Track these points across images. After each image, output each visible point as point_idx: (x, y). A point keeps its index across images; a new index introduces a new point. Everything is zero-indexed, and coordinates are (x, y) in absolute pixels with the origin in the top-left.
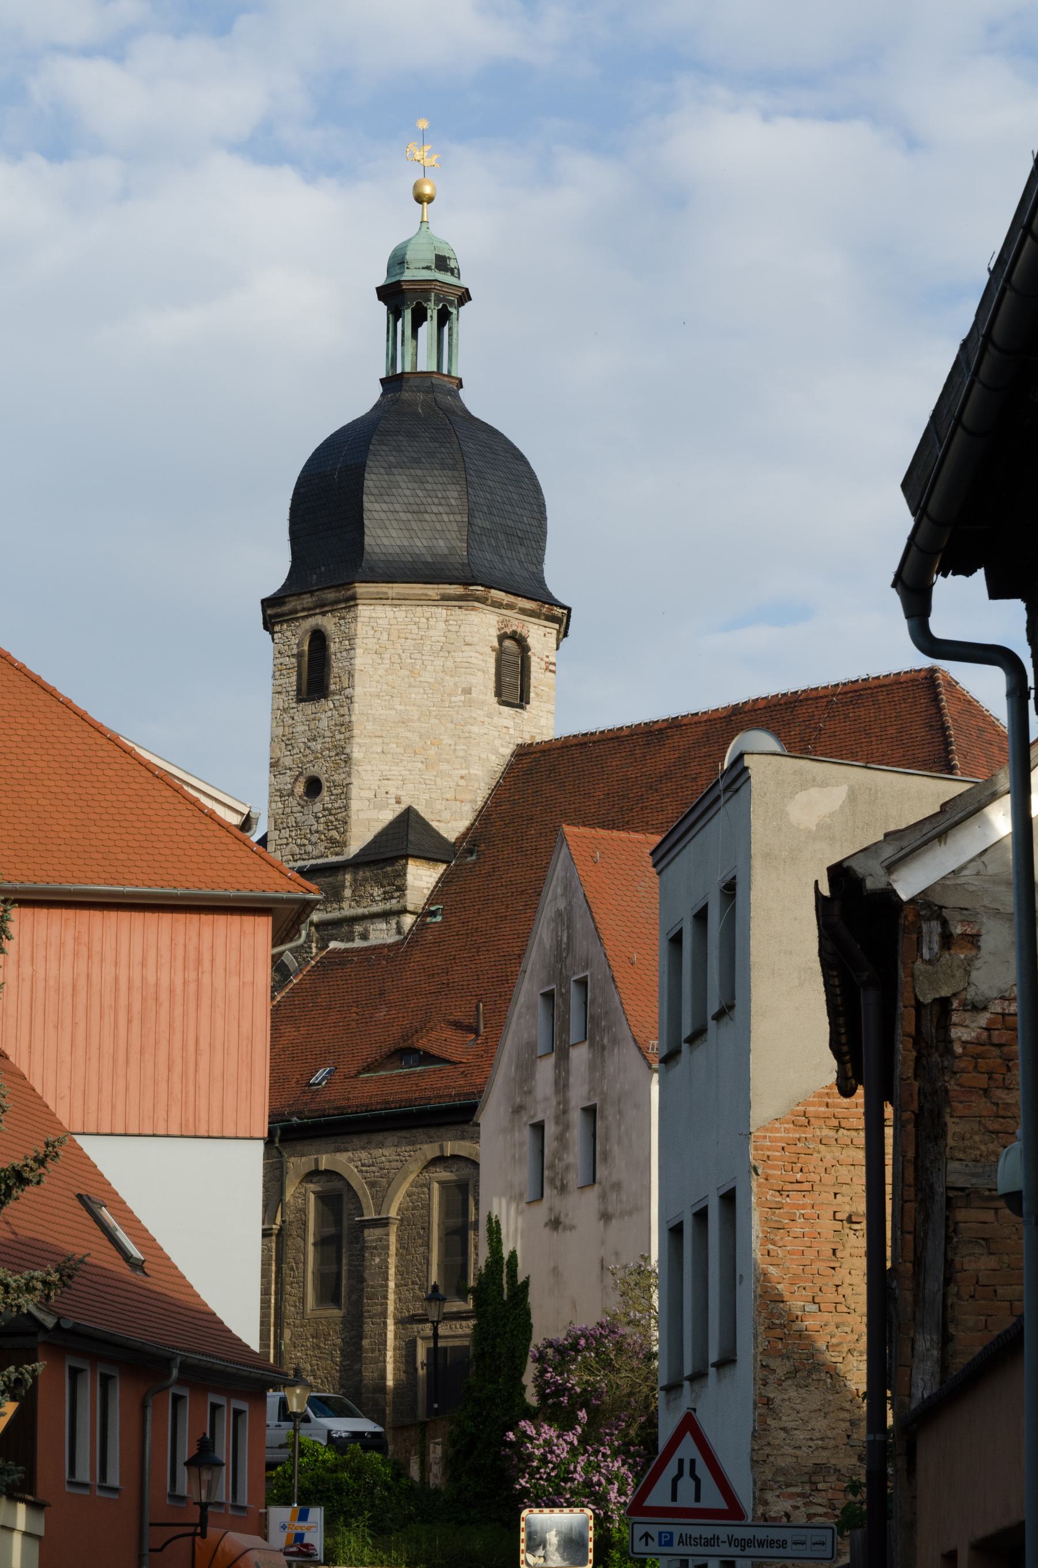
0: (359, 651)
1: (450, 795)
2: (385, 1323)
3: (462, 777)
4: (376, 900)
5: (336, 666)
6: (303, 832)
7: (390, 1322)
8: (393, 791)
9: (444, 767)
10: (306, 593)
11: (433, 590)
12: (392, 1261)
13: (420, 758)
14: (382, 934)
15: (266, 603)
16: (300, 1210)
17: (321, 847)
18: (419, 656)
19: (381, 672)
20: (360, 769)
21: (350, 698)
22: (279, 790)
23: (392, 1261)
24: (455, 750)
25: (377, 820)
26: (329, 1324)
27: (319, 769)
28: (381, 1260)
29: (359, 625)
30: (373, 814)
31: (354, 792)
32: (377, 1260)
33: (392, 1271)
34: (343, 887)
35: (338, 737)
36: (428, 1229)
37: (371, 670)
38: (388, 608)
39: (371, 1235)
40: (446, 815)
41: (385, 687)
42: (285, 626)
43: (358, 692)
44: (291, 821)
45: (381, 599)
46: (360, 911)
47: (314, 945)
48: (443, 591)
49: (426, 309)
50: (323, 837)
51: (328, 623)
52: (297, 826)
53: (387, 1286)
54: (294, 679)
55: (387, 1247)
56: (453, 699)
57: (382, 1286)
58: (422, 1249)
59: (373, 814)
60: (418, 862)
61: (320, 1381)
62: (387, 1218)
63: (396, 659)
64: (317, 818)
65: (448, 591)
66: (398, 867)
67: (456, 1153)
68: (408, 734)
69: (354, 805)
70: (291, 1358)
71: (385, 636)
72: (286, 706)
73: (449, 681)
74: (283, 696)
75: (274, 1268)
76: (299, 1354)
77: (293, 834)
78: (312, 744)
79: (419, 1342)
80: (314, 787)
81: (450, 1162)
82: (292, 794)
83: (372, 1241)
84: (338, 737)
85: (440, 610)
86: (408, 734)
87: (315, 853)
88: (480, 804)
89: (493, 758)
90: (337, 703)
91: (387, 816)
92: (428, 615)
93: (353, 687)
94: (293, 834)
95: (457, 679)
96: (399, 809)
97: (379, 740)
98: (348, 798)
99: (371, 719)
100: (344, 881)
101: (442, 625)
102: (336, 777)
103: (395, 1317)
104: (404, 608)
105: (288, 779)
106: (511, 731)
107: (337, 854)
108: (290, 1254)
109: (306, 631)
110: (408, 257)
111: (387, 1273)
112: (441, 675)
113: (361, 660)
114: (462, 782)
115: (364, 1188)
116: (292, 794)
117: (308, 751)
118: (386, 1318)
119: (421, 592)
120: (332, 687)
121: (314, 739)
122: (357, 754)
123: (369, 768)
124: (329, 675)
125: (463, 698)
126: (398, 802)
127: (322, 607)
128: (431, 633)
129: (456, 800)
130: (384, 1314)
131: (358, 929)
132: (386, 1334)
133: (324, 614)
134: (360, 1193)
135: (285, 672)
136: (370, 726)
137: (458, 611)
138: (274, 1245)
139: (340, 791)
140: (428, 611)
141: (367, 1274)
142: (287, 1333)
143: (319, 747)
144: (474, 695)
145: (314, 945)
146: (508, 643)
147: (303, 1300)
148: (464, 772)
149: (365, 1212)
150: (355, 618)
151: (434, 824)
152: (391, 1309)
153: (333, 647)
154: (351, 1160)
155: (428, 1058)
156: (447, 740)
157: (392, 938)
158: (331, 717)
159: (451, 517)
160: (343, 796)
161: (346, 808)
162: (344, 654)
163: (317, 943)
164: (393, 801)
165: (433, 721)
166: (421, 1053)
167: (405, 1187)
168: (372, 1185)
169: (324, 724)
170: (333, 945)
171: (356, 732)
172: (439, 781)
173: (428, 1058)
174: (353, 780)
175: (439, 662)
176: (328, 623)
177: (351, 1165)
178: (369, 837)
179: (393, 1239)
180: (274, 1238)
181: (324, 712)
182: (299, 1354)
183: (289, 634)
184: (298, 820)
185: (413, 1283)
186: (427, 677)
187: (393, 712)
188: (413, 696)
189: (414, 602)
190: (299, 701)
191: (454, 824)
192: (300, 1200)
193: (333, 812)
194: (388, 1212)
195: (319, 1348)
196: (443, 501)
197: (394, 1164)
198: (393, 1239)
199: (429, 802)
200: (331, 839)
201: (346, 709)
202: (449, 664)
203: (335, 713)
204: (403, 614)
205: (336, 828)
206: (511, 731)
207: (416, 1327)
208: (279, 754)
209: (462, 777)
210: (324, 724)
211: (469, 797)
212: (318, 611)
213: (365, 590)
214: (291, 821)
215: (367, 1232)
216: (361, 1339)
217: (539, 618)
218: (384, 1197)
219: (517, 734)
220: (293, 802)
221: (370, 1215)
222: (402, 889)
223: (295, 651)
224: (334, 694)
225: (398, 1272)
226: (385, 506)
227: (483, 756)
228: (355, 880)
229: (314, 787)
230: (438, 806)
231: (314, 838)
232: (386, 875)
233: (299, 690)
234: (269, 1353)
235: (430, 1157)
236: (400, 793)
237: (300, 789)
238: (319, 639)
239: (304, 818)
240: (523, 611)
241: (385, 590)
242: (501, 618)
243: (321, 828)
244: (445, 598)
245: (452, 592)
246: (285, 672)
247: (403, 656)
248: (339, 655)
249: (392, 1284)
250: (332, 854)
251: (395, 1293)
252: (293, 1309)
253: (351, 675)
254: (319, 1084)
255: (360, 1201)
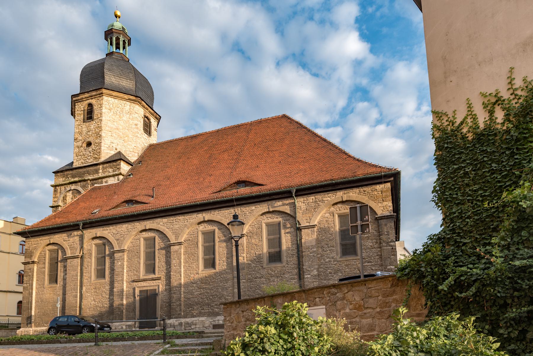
0: (104, 108)
1: (132, 150)
2: (123, 283)
3: (135, 146)
4: (111, 171)
5: (96, 112)
6: (85, 156)
7: (125, 282)
8: (114, 146)
9: (130, 143)
10: (86, 92)
11: (126, 97)
12: (125, 263)
13: (123, 139)
14: (112, 181)
15: (73, 96)
16: (89, 250)
17: (92, 160)
18: (122, 113)
19: (111, 115)
20: (104, 139)
21: (101, 120)
22: (77, 146)
23: (125, 263)
24: (133, 139)
25: (110, 153)
26: (100, 284)
27: (91, 139)
28: (121, 263)
29: (104, 101)
30: (109, 151)
31: (102, 144)
32: (120, 263)
33: (125, 267)
34: (99, 170)
35: (97, 130)
36: (139, 253)
37: (107, 114)
38: (113, 99)
39: (117, 255)
40: (130, 155)
41: (112, 119)
42: (79, 103)
43: (103, 118)
44: (81, 154)
45: (110, 95)
46: (105, 175)
47: (89, 186)
48: (129, 97)
49: (119, 39)
50: (92, 157)
51: (93, 101)
52: (84, 155)
53: (124, 271)
54: (82, 116)
55: (124, 259)
56: (132, 126)
57: (121, 271)
58: (137, 259)
59: (109, 151)
60: (124, 162)
61: (97, 303)
62: (124, 249)
63: (115, 112)
64: (90, 152)
65: (131, 97)
66: (118, 162)
67: (151, 228)
68: (119, 132)
69: (103, 148)
70: (86, 296)
71: (111, 106)
72: (80, 124)
73: (131, 122)
74: (79, 121)
75: (79, 268)
76: (89, 295)
77: (82, 157)
78: (88, 133)
79: (136, 288)
80: (89, 144)
81: (148, 231)
82: (82, 146)
83: (117, 257)
84: (97, 130)
85: (128, 102)
86: (119, 132)
87: (90, 161)
88: (140, 155)
89: (143, 145)
90: (96, 122)
91: (113, 153)
92: (125, 103)
93: (102, 117)
94: (82, 157)
95: (133, 121)
96: (116, 152)
97: (111, 132)
98: (101, 146)
99: (107, 126)
100: (99, 168)
101: (128, 107)
102: (96, 141)
103: (126, 281)
104: (117, 100)
105: (80, 143)
106: (147, 140)
107: (97, 161)
108: (85, 264)
109: (86, 104)
110: (114, 24)
111: (124, 267)
112: (128, 119)
113: (104, 110)
114: (135, 148)
115: (114, 241)
116: (82, 146)
117: (87, 135)
118: (123, 281)
119: (123, 96)
120: (95, 118)
121: (89, 132)
122: (103, 135)
123: (107, 139)
124: (94, 114)
125: (135, 126)
126: (116, 149)
127: (91, 97)
128: (125, 108)
129: (133, 152)
130: (123, 280)
131: (104, 180)
132: (123, 287)
133: (92, 99)
134: (113, 243)
135: (79, 115)
136: (107, 128)
137: (133, 104)
138: (79, 261)
139: (98, 144)
140: (125, 102)
141: (115, 268)
142: (84, 288)
143: (91, 133)
144: (138, 126)
145: (89, 186)
146: (146, 119)
147: (90, 278)
148: (135, 145)
149: (115, 248)
150: (102, 99)
151: (127, 157)
152: (125, 278)
153: (95, 107)
154: (109, 233)
155: (137, 202)
156: (130, 136)
157: (116, 182)
158: (95, 126)
159: (131, 81)
160: (99, 146)
161: (100, 149)
162: (99, 109)
163: (90, 185)
164: (115, 149)
165: (126, 130)
166: (134, 201)
167: (130, 240)
168: (117, 240)
169: (92, 127)
170: (96, 185)
171: (103, 129)
172: (128, 146)
173: (137, 202)
174: (102, 141)
175: (128, 116)
176: (93, 101)
177: (109, 234)
178: (107, 157)
179: (125, 256)
180: (79, 259)
181: (93, 125)
182: (89, 295)
183: (80, 105)
184: (84, 153)
185: (133, 270)
186: (124, 118)
187: (114, 126)
188: (120, 123)
189: (120, 99)
190: (84, 122)
191: (133, 158)
192: (89, 247)
193: (96, 150)
194: (124, 248)
195: (97, 292)
196: (128, 77)
197: (126, 233)
198: (125, 256)
199: (125, 151)
200: (95, 157)
201: (99, 123)
202: (131, 117)
203: (96, 124)
204: (117, 101)
205: (97, 154)
206: (147, 140)
207: (135, 283)
208: (77, 136)
209: (135, 146)
210: (92, 127)
211: (137, 152)
212: (90, 98)
213: (106, 91)
214: (81, 154)
215: (115, 255)
216: (113, 288)
217: (153, 116)
218: (122, 244)
219: (149, 142)
220: (82, 149)
221: (116, 248)
222: (119, 169)
223: (82, 109)
224: (95, 119)
225: (128, 267)
226: (111, 74)
227: (141, 143)
228: (103, 168)
229: (89, 144)
230: (128, 152)
231: (89, 158)
232: (113, 165)
233: (84, 119)
234: (77, 295)
235: (140, 229)
236: (117, 147)
237: (85, 145)
238: (90, 105)
239: (85, 153)
240: (150, 112)
241: (112, 93)
242: (145, 111)
243: (91, 155)
244: (129, 99)
245: (132, 98)
246: (79, 115)
247: (117, 112)
248: (97, 109)
249: (125, 271)
250: (95, 161)
251: (126, 273)
252: (86, 281)
253: (101, 114)
254: (96, 213)
255: (113, 245)
